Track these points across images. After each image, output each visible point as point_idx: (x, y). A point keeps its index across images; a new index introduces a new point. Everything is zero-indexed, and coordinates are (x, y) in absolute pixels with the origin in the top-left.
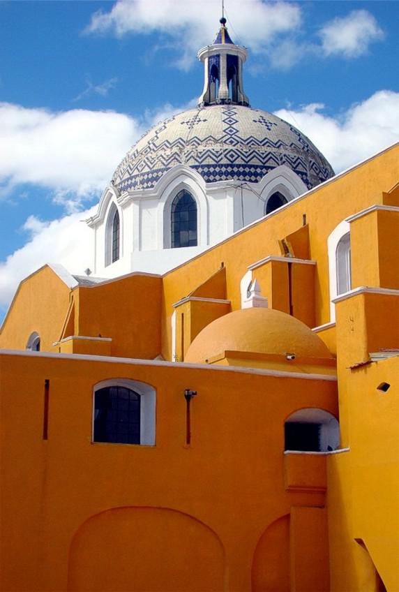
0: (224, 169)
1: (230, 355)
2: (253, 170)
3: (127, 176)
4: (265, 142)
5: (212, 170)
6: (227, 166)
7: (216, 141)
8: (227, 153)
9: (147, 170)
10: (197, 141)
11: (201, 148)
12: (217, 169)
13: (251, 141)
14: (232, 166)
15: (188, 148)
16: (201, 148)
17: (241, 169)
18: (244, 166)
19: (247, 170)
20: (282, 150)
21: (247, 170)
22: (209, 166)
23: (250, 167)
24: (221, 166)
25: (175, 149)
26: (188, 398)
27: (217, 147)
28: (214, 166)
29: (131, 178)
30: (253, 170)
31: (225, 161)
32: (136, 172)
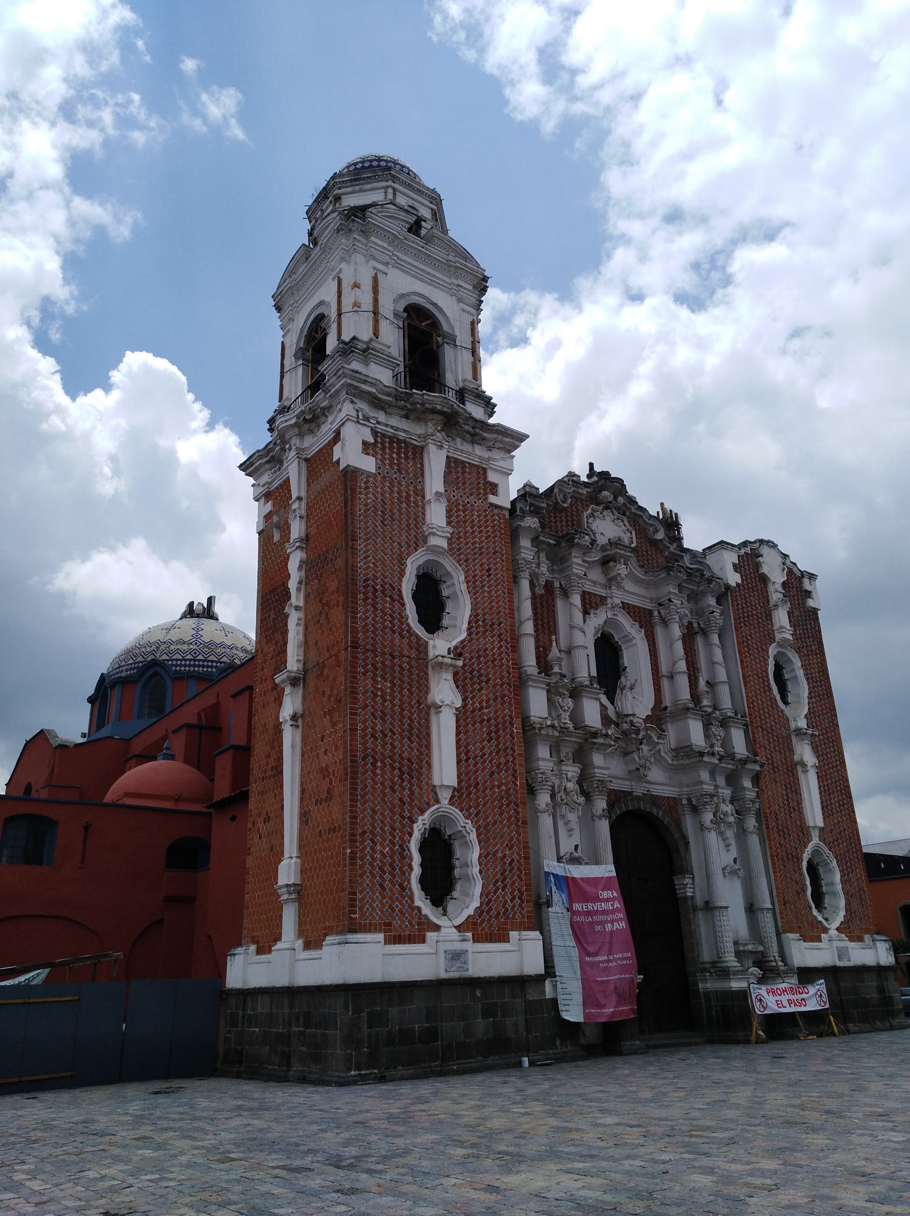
0: (188, 663)
1: (127, 795)
2: (210, 664)
3: (117, 666)
4: (222, 645)
5: (179, 663)
6: (190, 660)
7: (184, 643)
8: (190, 651)
9: (131, 661)
10: (171, 643)
11: (172, 647)
12: (183, 662)
13: (211, 643)
14: (195, 660)
15: (163, 647)
16: (172, 647)
17: (201, 663)
18: (203, 661)
19: (206, 663)
20: (234, 651)
21: (206, 663)
22: (177, 660)
23: (208, 661)
24: (186, 660)
25: (153, 647)
26: (86, 828)
27: (185, 647)
28: (181, 660)
29: (119, 667)
30: (210, 664)
31: (189, 657)
32: (123, 663)
